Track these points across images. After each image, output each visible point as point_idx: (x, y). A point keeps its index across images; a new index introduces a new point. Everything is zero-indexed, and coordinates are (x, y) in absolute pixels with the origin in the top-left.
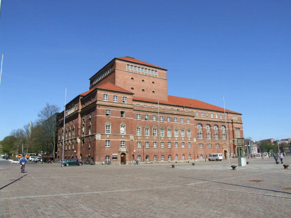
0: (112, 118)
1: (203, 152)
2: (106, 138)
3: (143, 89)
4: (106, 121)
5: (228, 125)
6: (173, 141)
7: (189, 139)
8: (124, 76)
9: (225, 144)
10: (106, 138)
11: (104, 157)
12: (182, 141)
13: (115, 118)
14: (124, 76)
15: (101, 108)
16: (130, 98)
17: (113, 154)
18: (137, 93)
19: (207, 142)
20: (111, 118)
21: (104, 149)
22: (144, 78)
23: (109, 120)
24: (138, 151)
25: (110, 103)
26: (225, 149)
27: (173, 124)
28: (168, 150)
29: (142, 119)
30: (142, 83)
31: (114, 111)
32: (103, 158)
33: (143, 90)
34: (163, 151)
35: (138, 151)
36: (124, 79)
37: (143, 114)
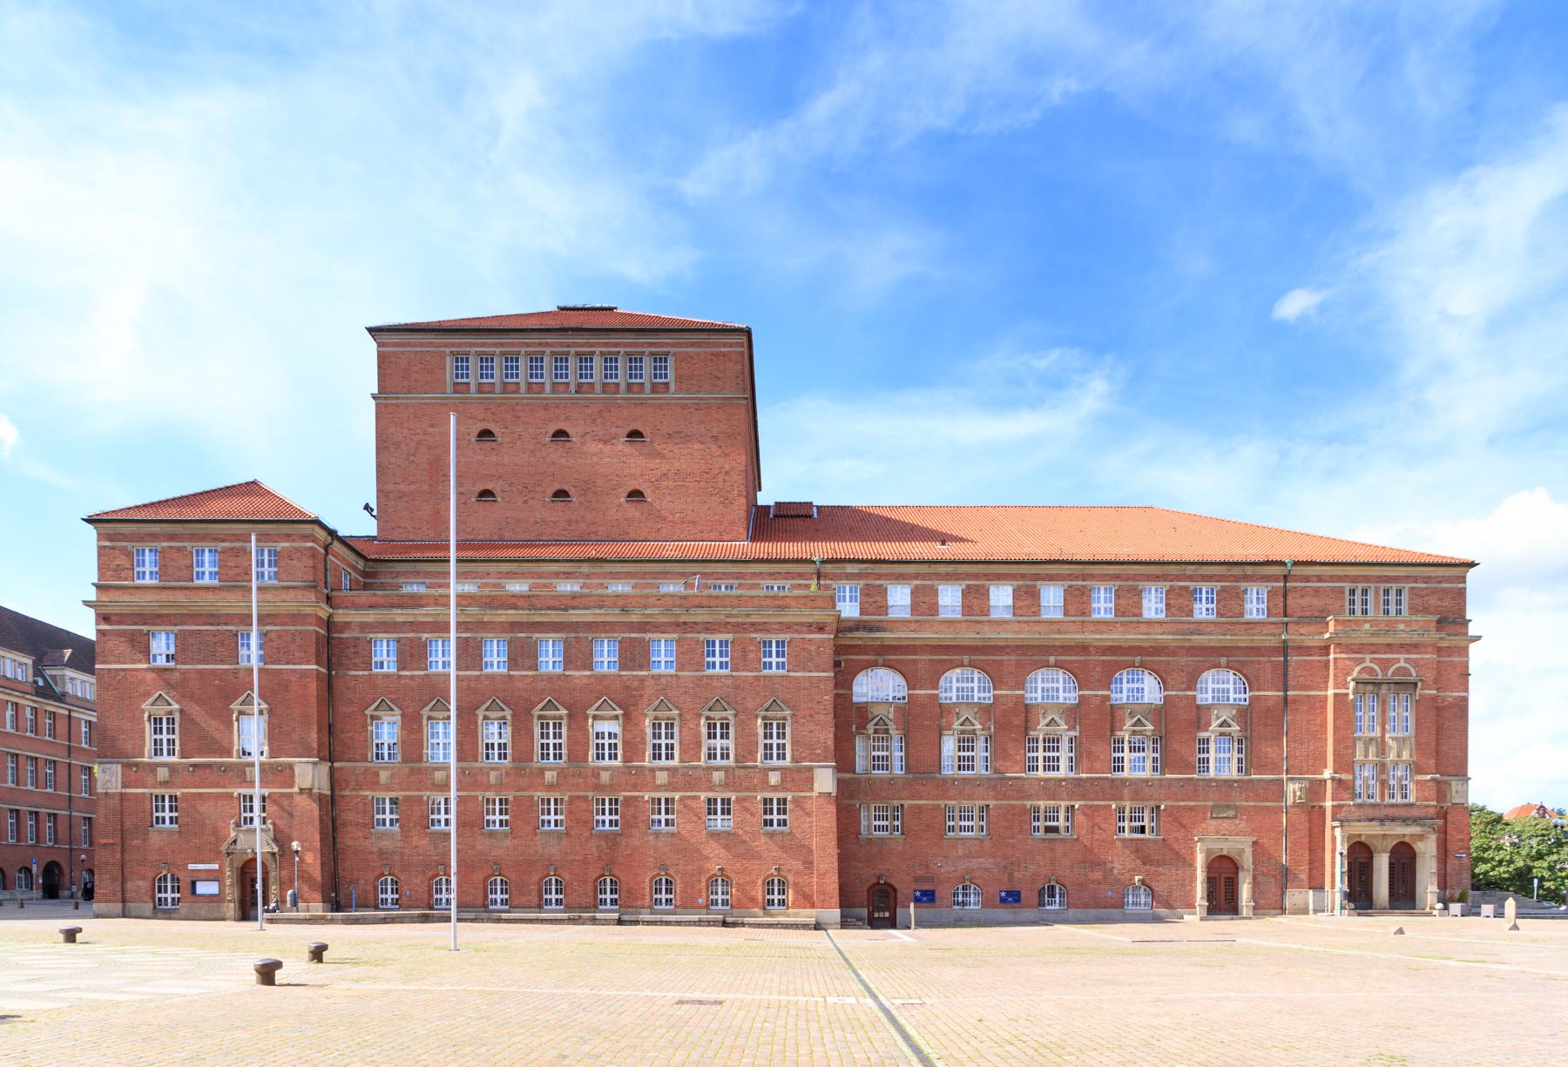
0: (184, 673)
1: (986, 862)
2: (150, 779)
3: (557, 487)
4: (147, 695)
5: (1286, 661)
6: (635, 787)
7: (774, 778)
8: (430, 430)
9: (1231, 813)
10: (150, 779)
11: (144, 878)
12: (711, 789)
13: (199, 672)
14: (432, 426)
15: (120, 623)
16: (299, 550)
17: (191, 867)
18: (519, 521)
19: (1029, 797)
20: (177, 675)
21: (145, 840)
22: (568, 418)
23: (170, 686)
24: (375, 850)
25: (167, 592)
26: (1226, 847)
27: (642, 679)
28: (593, 843)
29: (404, 669)
30: (556, 453)
31: (192, 633)
32: (140, 883)
33: (561, 494)
34: (554, 850)
35: (375, 850)
36: (430, 448)
37: (411, 640)
